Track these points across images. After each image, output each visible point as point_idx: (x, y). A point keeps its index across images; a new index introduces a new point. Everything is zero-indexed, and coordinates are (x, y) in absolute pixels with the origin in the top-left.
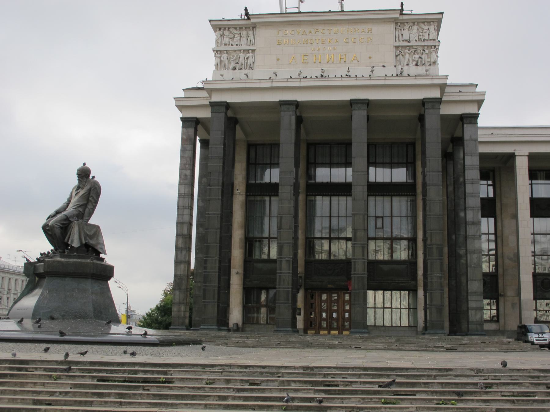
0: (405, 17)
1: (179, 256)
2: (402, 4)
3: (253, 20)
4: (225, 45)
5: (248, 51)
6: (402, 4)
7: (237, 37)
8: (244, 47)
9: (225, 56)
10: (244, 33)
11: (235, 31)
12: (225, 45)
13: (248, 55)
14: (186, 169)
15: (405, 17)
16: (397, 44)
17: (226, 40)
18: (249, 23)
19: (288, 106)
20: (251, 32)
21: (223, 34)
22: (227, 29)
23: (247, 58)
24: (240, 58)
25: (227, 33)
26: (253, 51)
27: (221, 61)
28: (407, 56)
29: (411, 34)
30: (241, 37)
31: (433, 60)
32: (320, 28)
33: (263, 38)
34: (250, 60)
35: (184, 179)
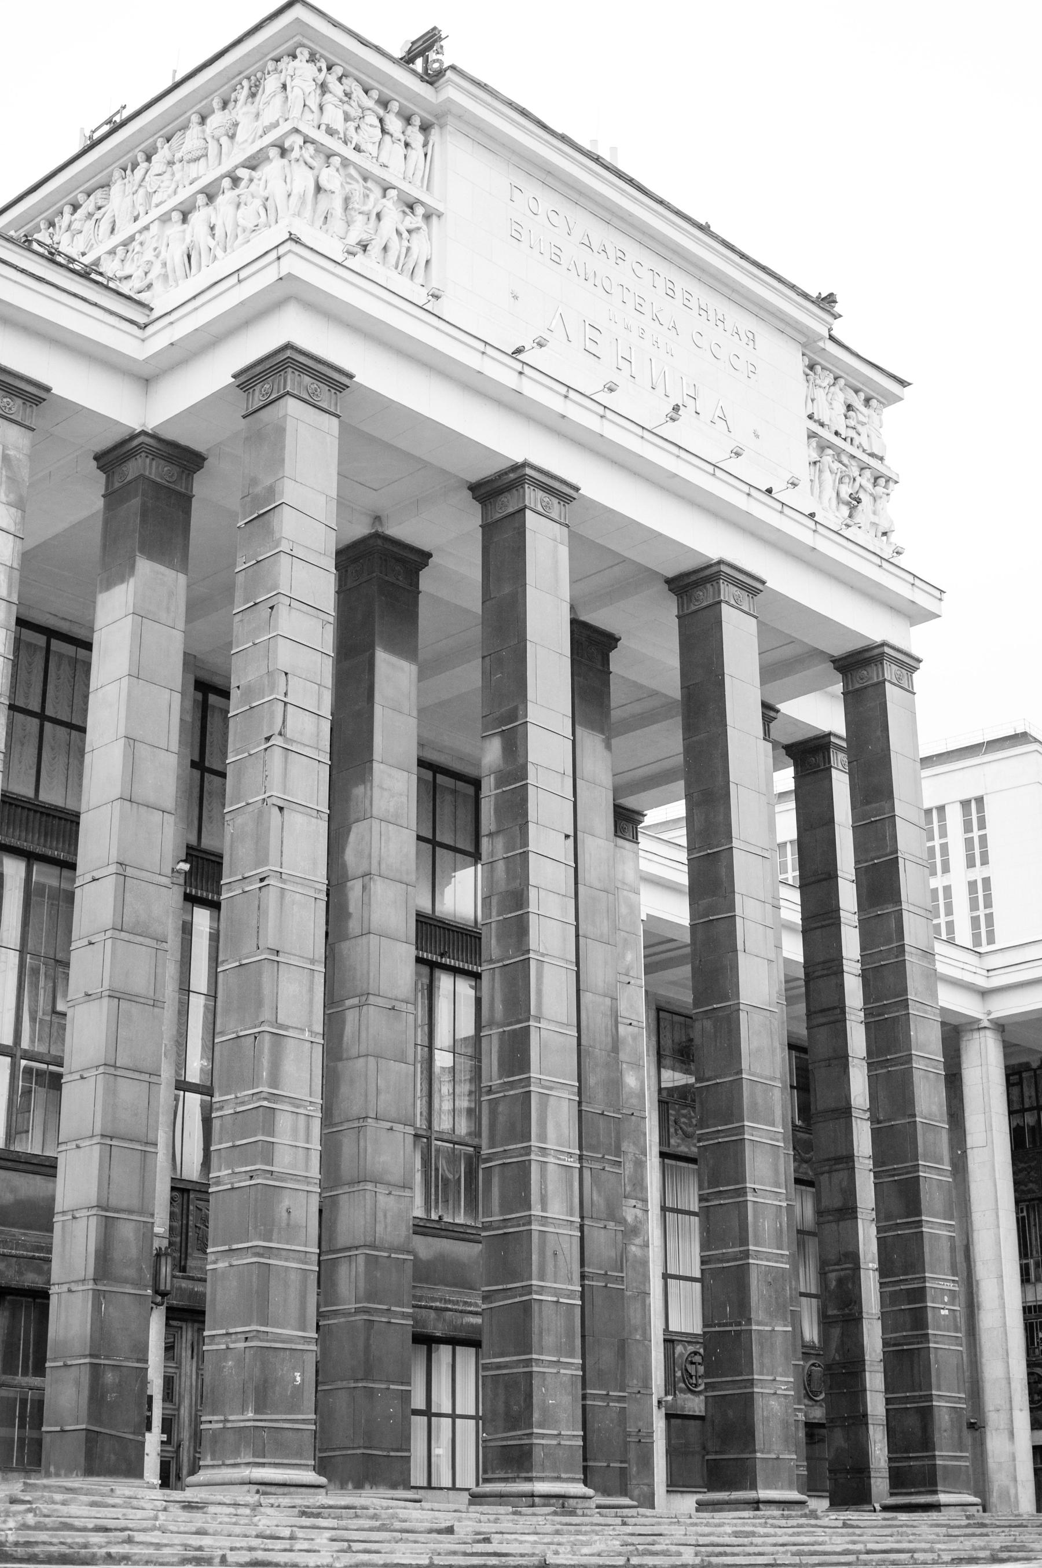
3: (451, 92)
4: (331, 132)
10: (395, 124)
11: (358, 92)
12: (331, 132)
13: (415, 220)
15: (831, 347)
16: (816, 428)
17: (334, 116)
19: (546, 498)
20: (416, 137)
21: (323, 87)
22: (338, 71)
24: (378, 216)
27: (318, 189)
28: (828, 478)
30: (384, 131)
31: (884, 527)
34: (420, 246)
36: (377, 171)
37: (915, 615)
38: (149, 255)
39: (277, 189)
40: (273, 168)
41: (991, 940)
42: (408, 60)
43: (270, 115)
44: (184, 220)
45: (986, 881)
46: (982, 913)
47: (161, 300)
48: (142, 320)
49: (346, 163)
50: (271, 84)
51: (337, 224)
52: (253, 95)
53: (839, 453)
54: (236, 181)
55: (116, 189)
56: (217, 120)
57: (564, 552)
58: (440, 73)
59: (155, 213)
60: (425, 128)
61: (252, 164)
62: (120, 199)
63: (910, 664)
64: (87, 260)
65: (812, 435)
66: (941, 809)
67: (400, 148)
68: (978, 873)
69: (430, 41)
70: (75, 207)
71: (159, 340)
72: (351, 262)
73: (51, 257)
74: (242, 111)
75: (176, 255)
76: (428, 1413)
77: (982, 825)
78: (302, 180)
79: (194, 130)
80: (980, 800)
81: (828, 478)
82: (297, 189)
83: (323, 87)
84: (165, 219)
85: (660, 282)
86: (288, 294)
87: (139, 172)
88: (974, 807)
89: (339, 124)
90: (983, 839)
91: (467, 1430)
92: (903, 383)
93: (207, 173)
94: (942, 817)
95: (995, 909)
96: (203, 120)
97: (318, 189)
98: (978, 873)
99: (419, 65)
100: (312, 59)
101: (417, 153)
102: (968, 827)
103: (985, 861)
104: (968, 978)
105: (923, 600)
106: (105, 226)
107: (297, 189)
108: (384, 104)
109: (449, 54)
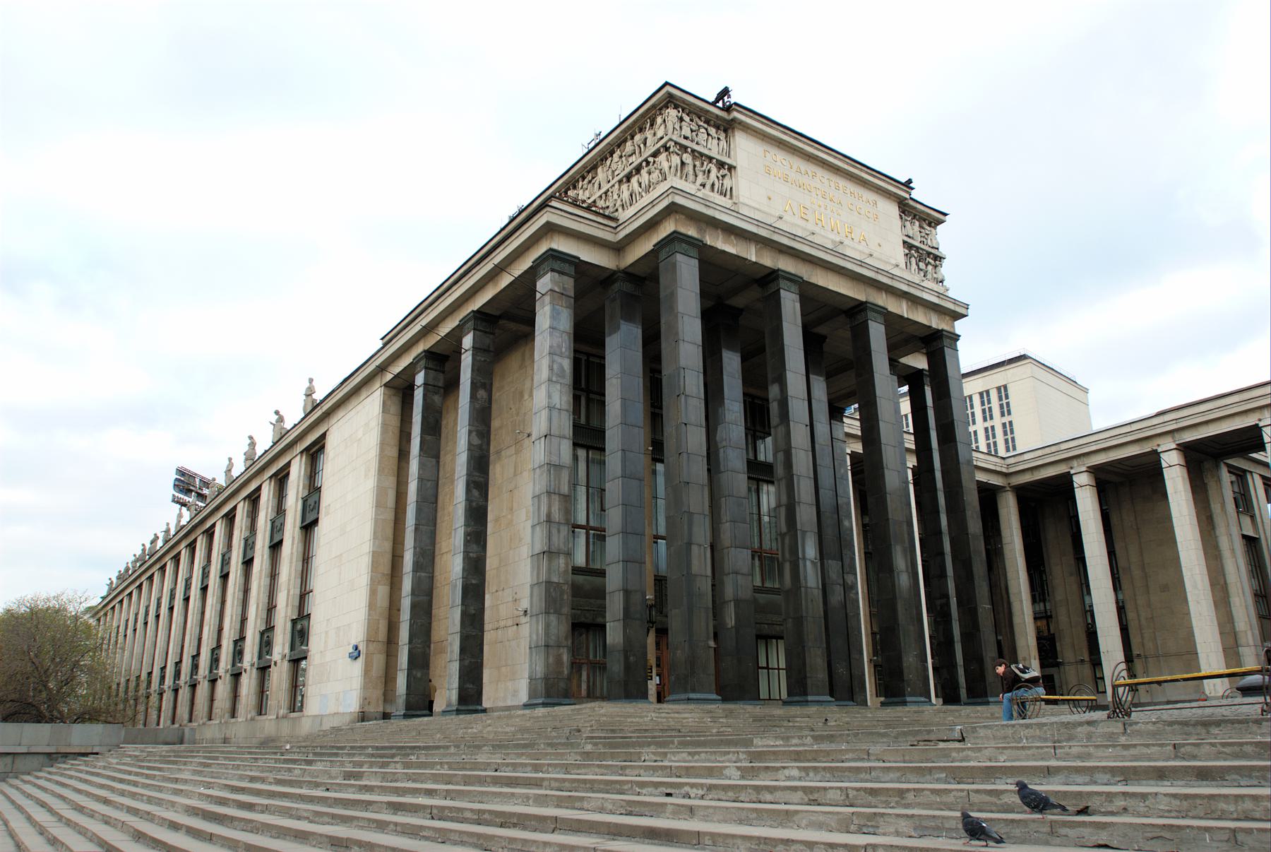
0: (911, 203)
1: (555, 539)
2: (910, 181)
4: (686, 138)
5: (721, 165)
6: (910, 181)
7: (702, 136)
8: (714, 154)
9: (687, 158)
10: (712, 131)
11: (696, 119)
12: (686, 138)
13: (723, 172)
14: (561, 355)
18: (724, 117)
20: (722, 136)
21: (681, 120)
23: (723, 176)
24: (709, 171)
25: (687, 118)
26: (731, 168)
27: (683, 163)
29: (914, 229)
32: (821, 173)
33: (744, 149)
34: (727, 183)
35: (558, 375)
36: (706, 152)
37: (958, 316)
38: (616, 197)
39: (665, 165)
40: (662, 157)
41: (1014, 449)
42: (714, 104)
43: (660, 133)
44: (628, 181)
45: (1011, 423)
46: (1009, 437)
47: (623, 215)
48: (614, 225)
49: (693, 151)
50: (659, 120)
51: (691, 177)
52: (652, 125)
53: (917, 249)
54: (648, 163)
55: (600, 170)
56: (638, 137)
57: (798, 305)
58: (730, 106)
59: (617, 179)
60: (725, 131)
61: (655, 155)
62: (601, 174)
63: (956, 337)
64: (589, 201)
65: (904, 242)
66: (988, 392)
67: (715, 141)
68: (1006, 419)
69: (725, 92)
70: (584, 179)
71: (622, 235)
72: (699, 194)
73: (575, 203)
74: (648, 134)
75: (626, 195)
76: (767, 668)
77: (1007, 397)
78: (676, 160)
79: (629, 143)
80: (1005, 387)
81: (913, 260)
82: (673, 165)
83: (681, 120)
84: (620, 182)
85: (832, 184)
86: (673, 209)
87: (608, 162)
88: (1003, 391)
89: (688, 134)
90: (1008, 404)
91: (783, 673)
92: (945, 215)
93: (636, 160)
94: (988, 395)
95: (1016, 435)
96: (632, 138)
97: (683, 163)
98: (1006, 419)
99: (720, 104)
100: (676, 107)
101: (723, 143)
102: (1000, 399)
103: (1009, 413)
104: (998, 469)
105: (962, 311)
106: (596, 185)
107: (673, 165)
108: (707, 122)
109: (734, 98)
